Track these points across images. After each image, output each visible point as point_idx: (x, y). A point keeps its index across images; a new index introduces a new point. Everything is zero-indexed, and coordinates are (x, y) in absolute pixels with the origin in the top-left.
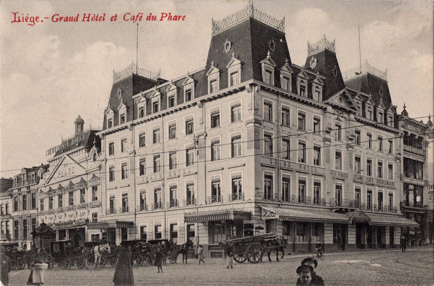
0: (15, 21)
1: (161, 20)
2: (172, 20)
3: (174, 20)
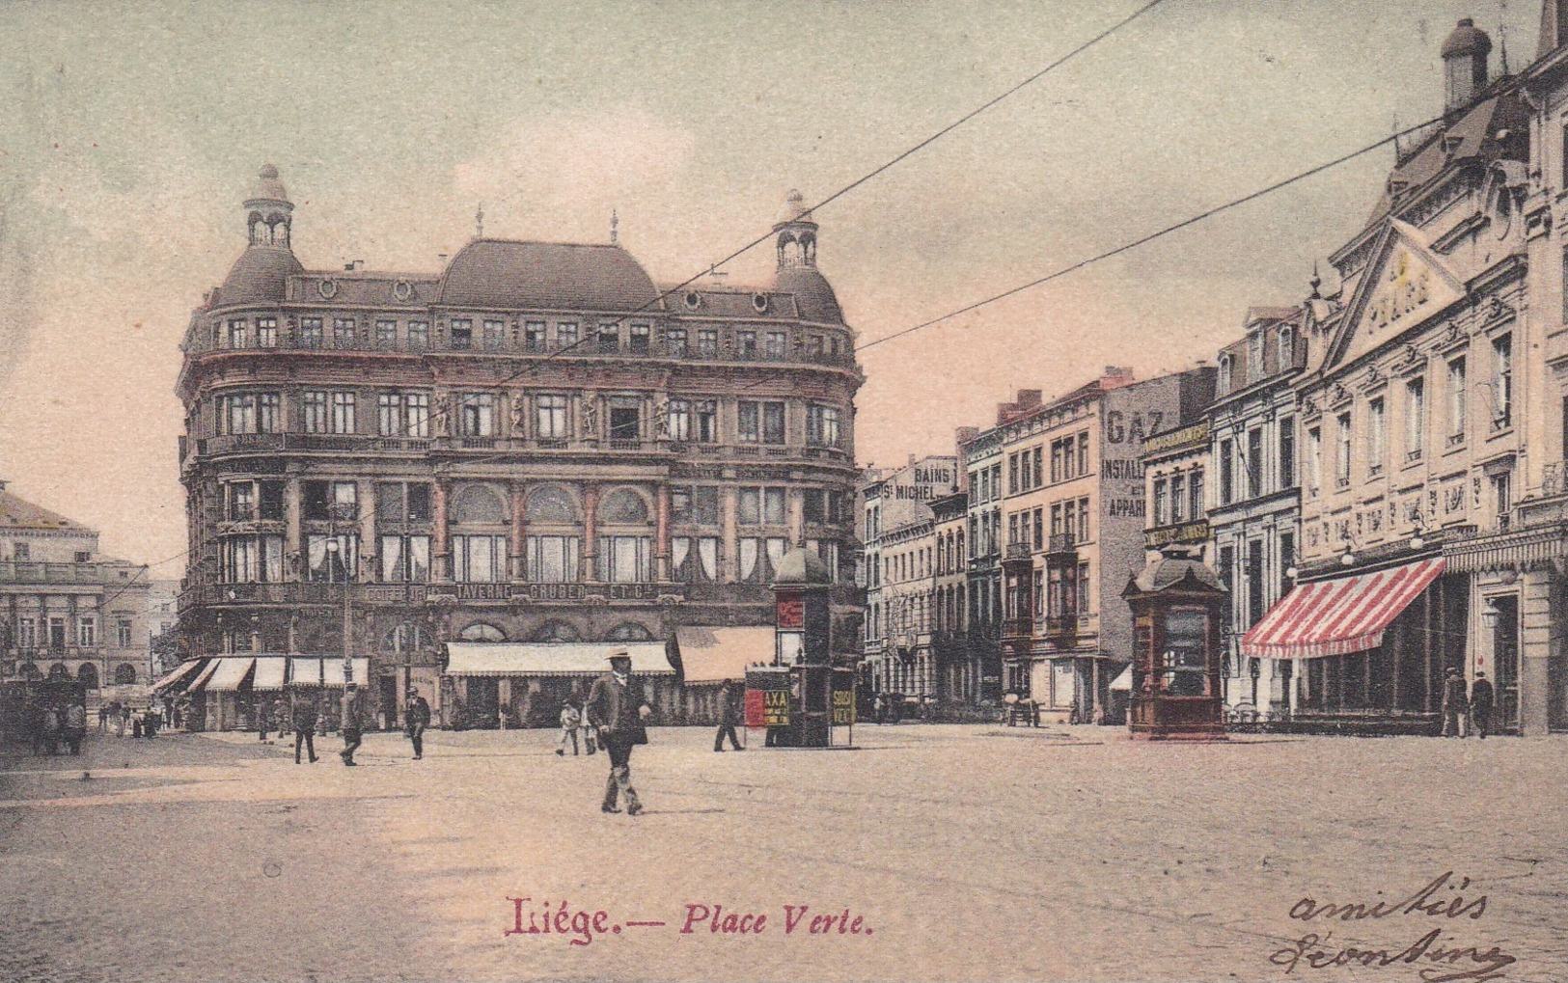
0: (518, 930)
1: (687, 930)
2: (848, 932)
3: (725, 930)
